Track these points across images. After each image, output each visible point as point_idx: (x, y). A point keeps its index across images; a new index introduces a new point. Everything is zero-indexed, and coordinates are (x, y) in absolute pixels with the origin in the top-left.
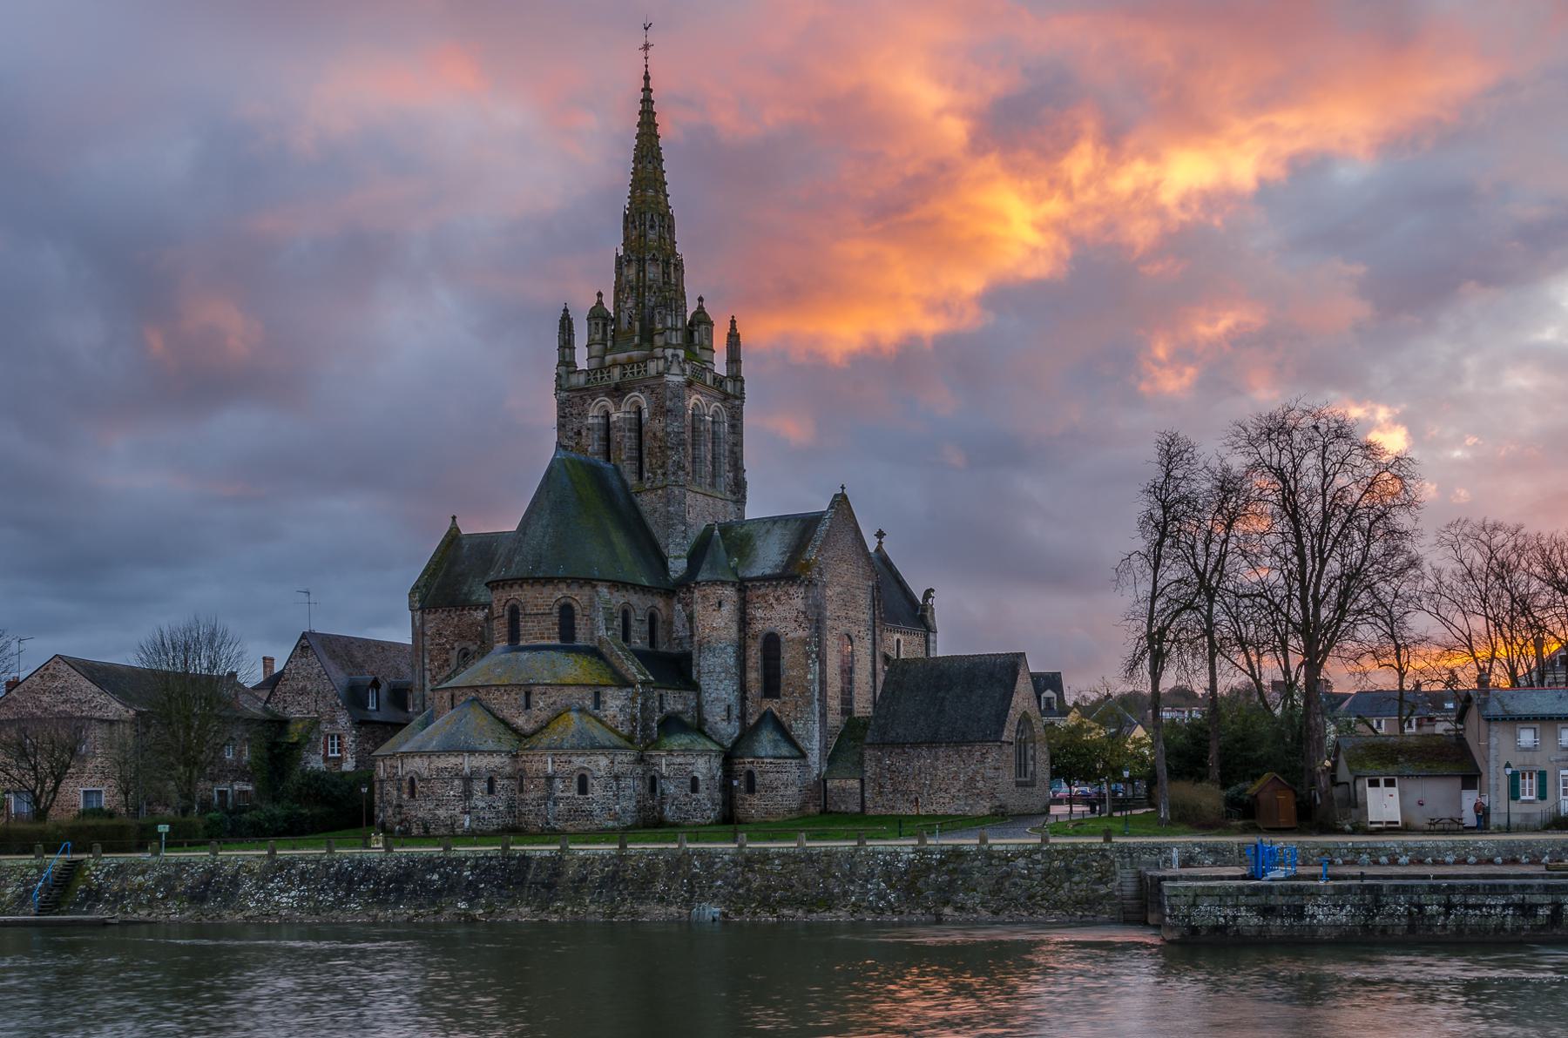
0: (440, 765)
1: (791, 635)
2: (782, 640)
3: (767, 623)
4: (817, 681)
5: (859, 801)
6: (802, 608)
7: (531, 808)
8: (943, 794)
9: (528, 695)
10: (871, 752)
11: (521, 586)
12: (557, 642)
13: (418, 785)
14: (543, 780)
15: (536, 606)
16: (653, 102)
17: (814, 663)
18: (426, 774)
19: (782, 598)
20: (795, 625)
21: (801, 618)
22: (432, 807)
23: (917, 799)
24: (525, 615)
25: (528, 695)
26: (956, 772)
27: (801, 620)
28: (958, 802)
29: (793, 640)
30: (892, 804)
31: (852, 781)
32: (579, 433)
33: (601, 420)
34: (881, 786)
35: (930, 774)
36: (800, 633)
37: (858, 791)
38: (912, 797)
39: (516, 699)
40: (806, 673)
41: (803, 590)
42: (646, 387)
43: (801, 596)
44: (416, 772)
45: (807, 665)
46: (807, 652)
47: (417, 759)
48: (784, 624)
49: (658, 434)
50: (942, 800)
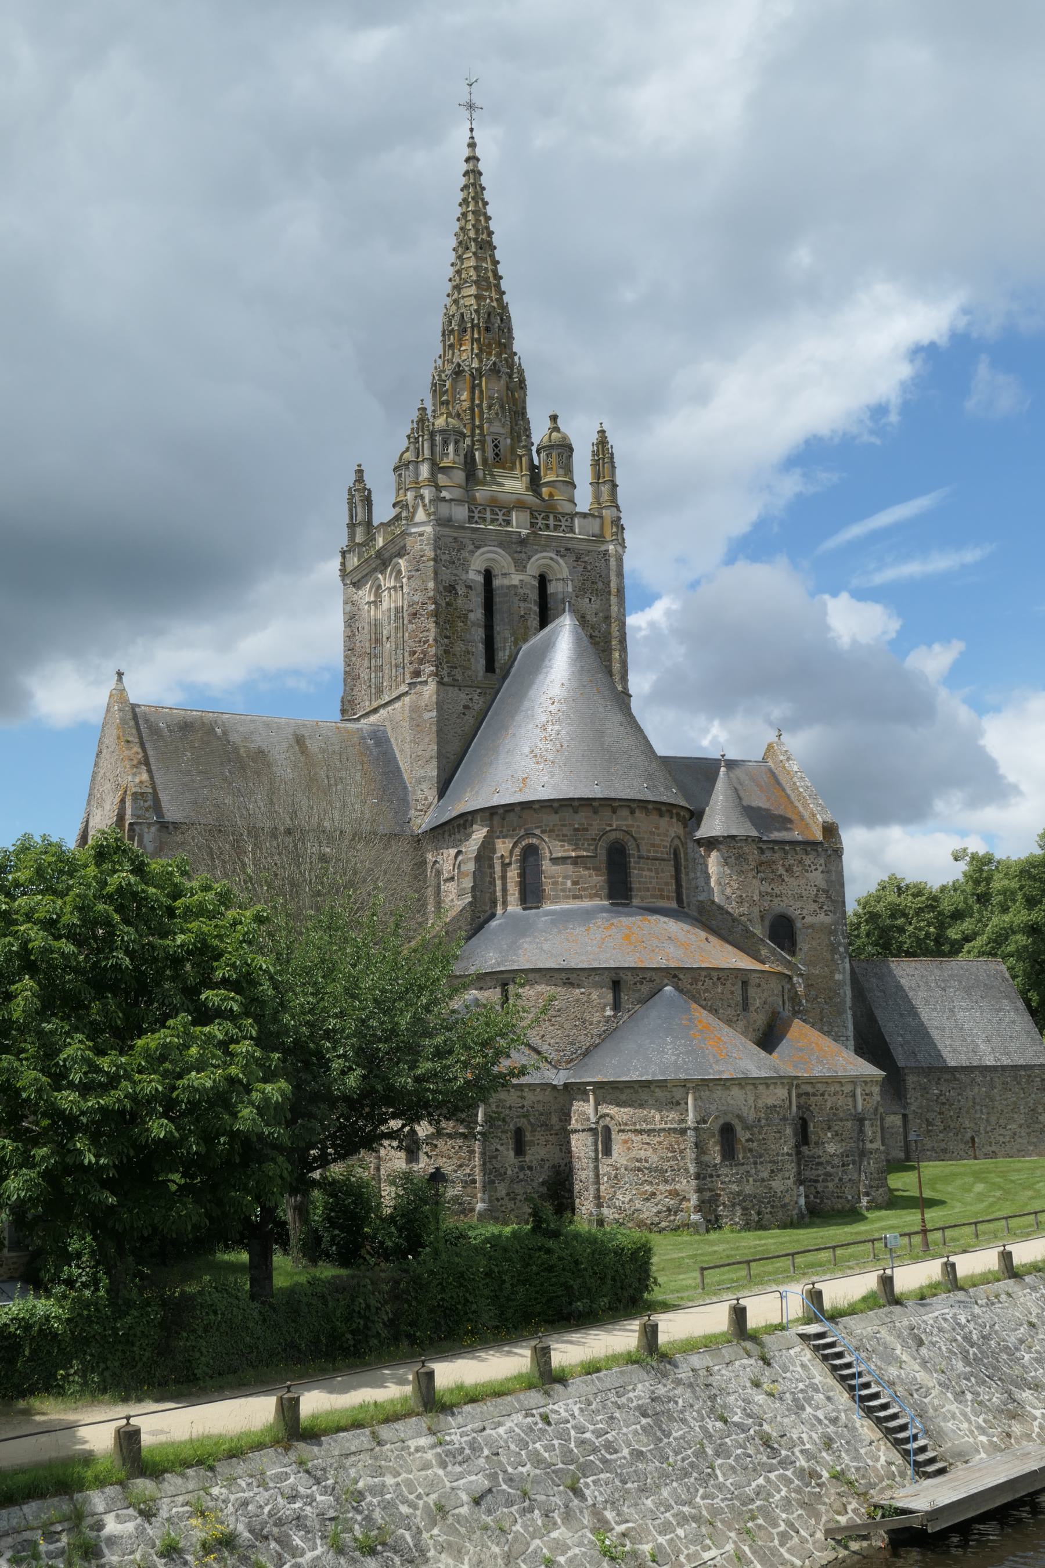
0: (770, 1102)
1: (809, 920)
2: (799, 924)
3: (776, 900)
4: (848, 982)
5: (902, 1144)
6: (823, 885)
7: (829, 1168)
8: (1002, 1131)
9: (745, 983)
10: (916, 1079)
11: (632, 812)
12: (674, 905)
13: (742, 1135)
14: (849, 1124)
15: (653, 845)
16: (480, 174)
17: (843, 959)
18: (751, 1116)
19: (795, 868)
20: (815, 906)
21: (822, 898)
22: (765, 1175)
23: (973, 1139)
24: (640, 857)
25: (745, 983)
26: (1015, 1103)
27: (821, 900)
28: (1020, 1140)
29: (812, 926)
30: (943, 1145)
31: (892, 1117)
32: (451, 589)
33: (480, 579)
34: (929, 1123)
35: (987, 1106)
36: (822, 917)
37: (901, 1130)
38: (968, 1135)
39: (732, 993)
40: (832, 972)
41: (822, 861)
42: (567, 549)
43: (820, 869)
44: (739, 1117)
45: (833, 960)
46: (832, 944)
47: (735, 1091)
48: (799, 904)
49: (588, 617)
50: (1002, 1139)
